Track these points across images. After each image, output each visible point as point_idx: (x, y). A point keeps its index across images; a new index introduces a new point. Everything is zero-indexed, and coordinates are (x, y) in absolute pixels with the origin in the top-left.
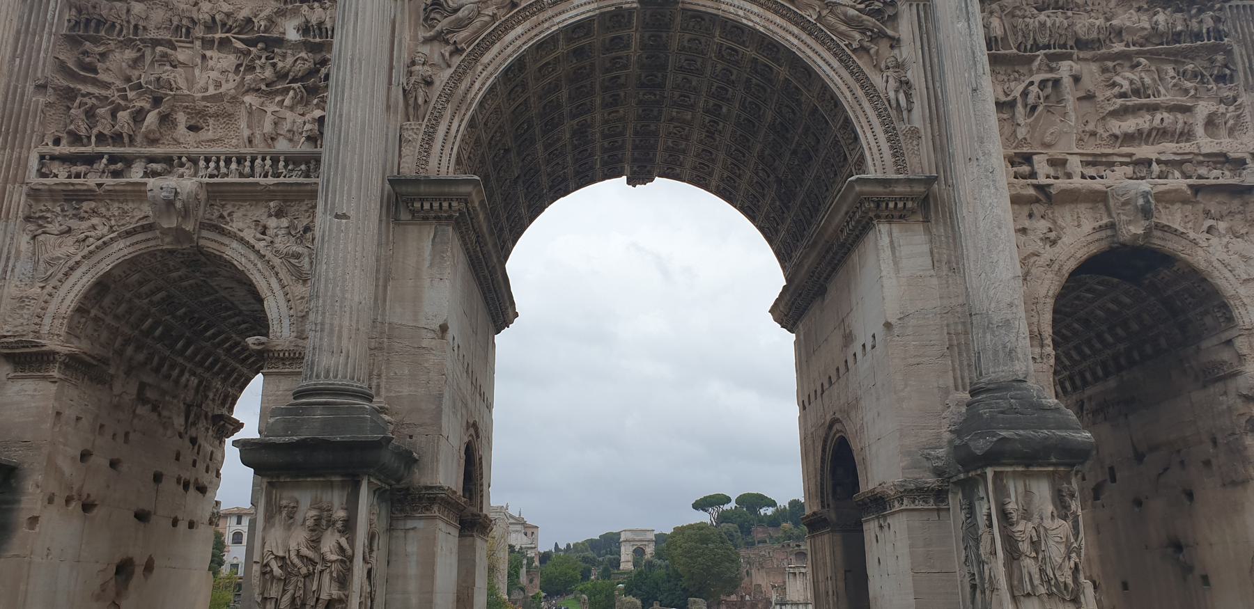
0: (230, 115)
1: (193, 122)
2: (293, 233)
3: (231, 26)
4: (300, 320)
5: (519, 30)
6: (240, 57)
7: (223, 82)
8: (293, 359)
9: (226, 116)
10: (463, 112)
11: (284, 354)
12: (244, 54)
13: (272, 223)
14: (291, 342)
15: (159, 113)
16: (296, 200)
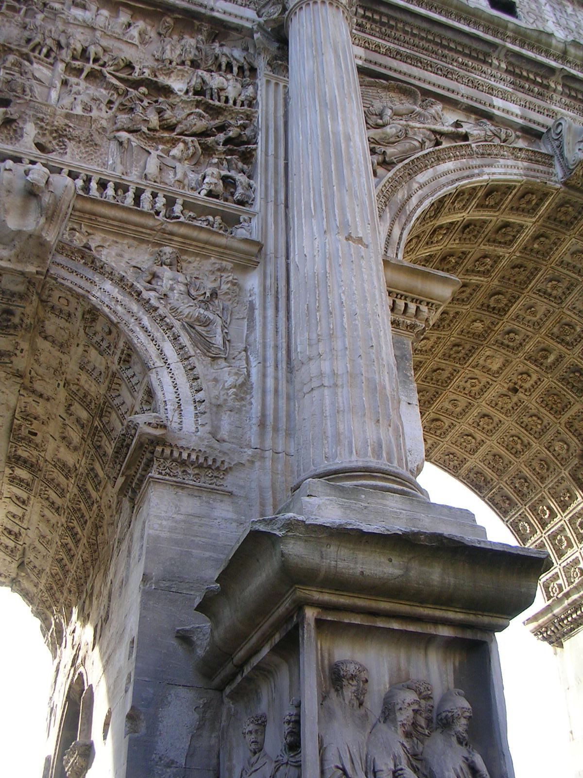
0: (96, 145)
1: (42, 140)
2: (193, 292)
3: (105, 63)
4: (215, 409)
5: (449, 165)
6: (113, 95)
7: (94, 107)
8: (200, 466)
9: (92, 145)
10: (404, 221)
11: (189, 455)
12: (119, 95)
13: (167, 273)
14: (201, 439)
15: (6, 113)
16: (197, 255)
